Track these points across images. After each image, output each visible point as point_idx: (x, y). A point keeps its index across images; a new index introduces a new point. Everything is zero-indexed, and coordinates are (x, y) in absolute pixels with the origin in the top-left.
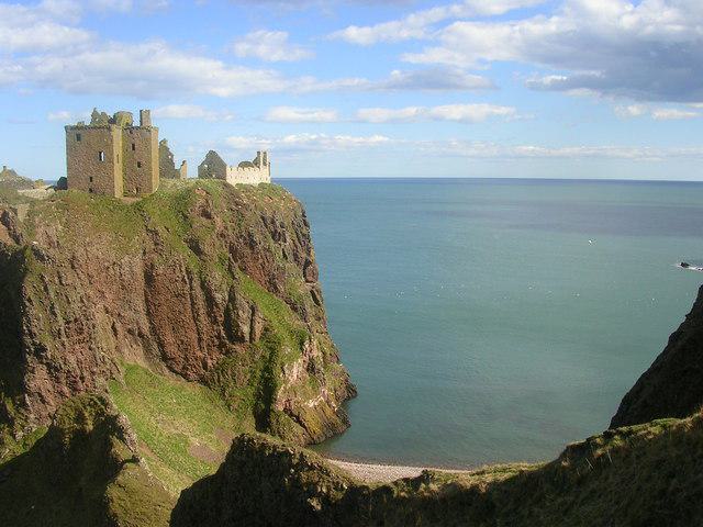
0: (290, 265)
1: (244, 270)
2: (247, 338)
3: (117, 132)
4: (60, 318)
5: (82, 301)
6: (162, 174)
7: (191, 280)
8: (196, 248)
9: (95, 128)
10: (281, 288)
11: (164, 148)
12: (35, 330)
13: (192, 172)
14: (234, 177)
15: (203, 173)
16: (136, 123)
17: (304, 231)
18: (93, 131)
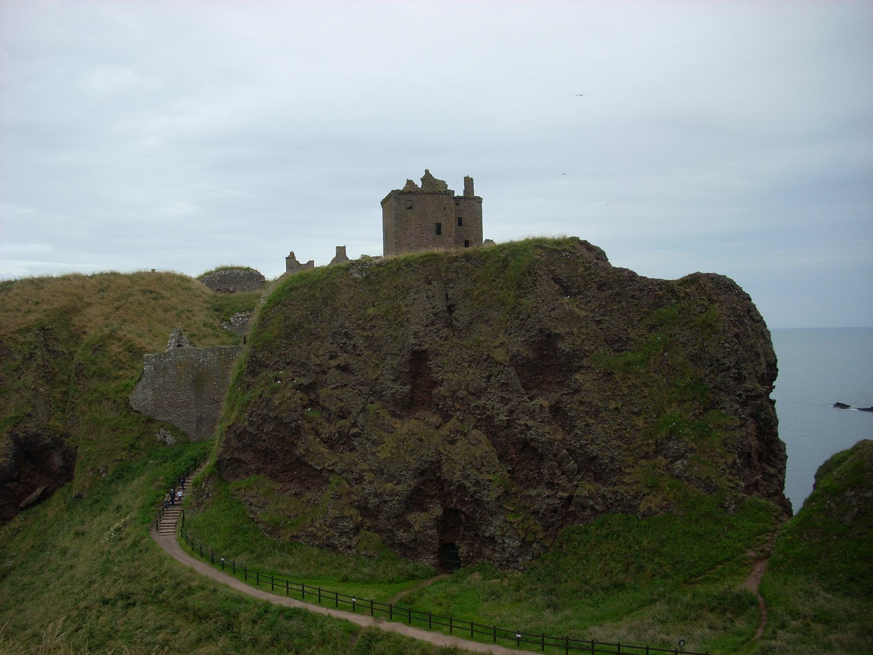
4: (762, 360)
16: (459, 192)
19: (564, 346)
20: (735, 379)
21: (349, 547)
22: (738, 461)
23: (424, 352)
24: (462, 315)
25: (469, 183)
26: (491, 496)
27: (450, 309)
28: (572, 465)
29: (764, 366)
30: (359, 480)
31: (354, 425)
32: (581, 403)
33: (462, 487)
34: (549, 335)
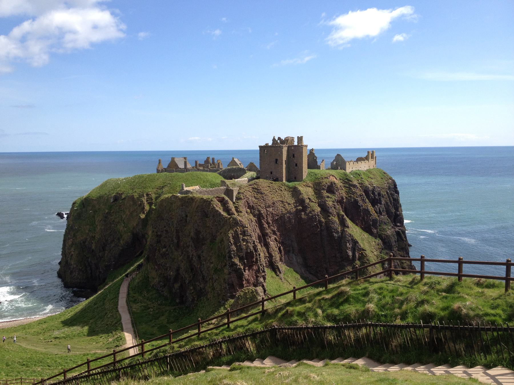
0: (384, 217)
2: (351, 257)
9: (274, 147)
10: (375, 231)
14: (350, 168)
15: (334, 167)
16: (296, 143)
17: (395, 197)
18: (273, 149)
20: (229, 257)
24: (188, 218)
25: (300, 139)
26: (187, 282)
30: (167, 269)
31: (167, 250)
32: (203, 257)
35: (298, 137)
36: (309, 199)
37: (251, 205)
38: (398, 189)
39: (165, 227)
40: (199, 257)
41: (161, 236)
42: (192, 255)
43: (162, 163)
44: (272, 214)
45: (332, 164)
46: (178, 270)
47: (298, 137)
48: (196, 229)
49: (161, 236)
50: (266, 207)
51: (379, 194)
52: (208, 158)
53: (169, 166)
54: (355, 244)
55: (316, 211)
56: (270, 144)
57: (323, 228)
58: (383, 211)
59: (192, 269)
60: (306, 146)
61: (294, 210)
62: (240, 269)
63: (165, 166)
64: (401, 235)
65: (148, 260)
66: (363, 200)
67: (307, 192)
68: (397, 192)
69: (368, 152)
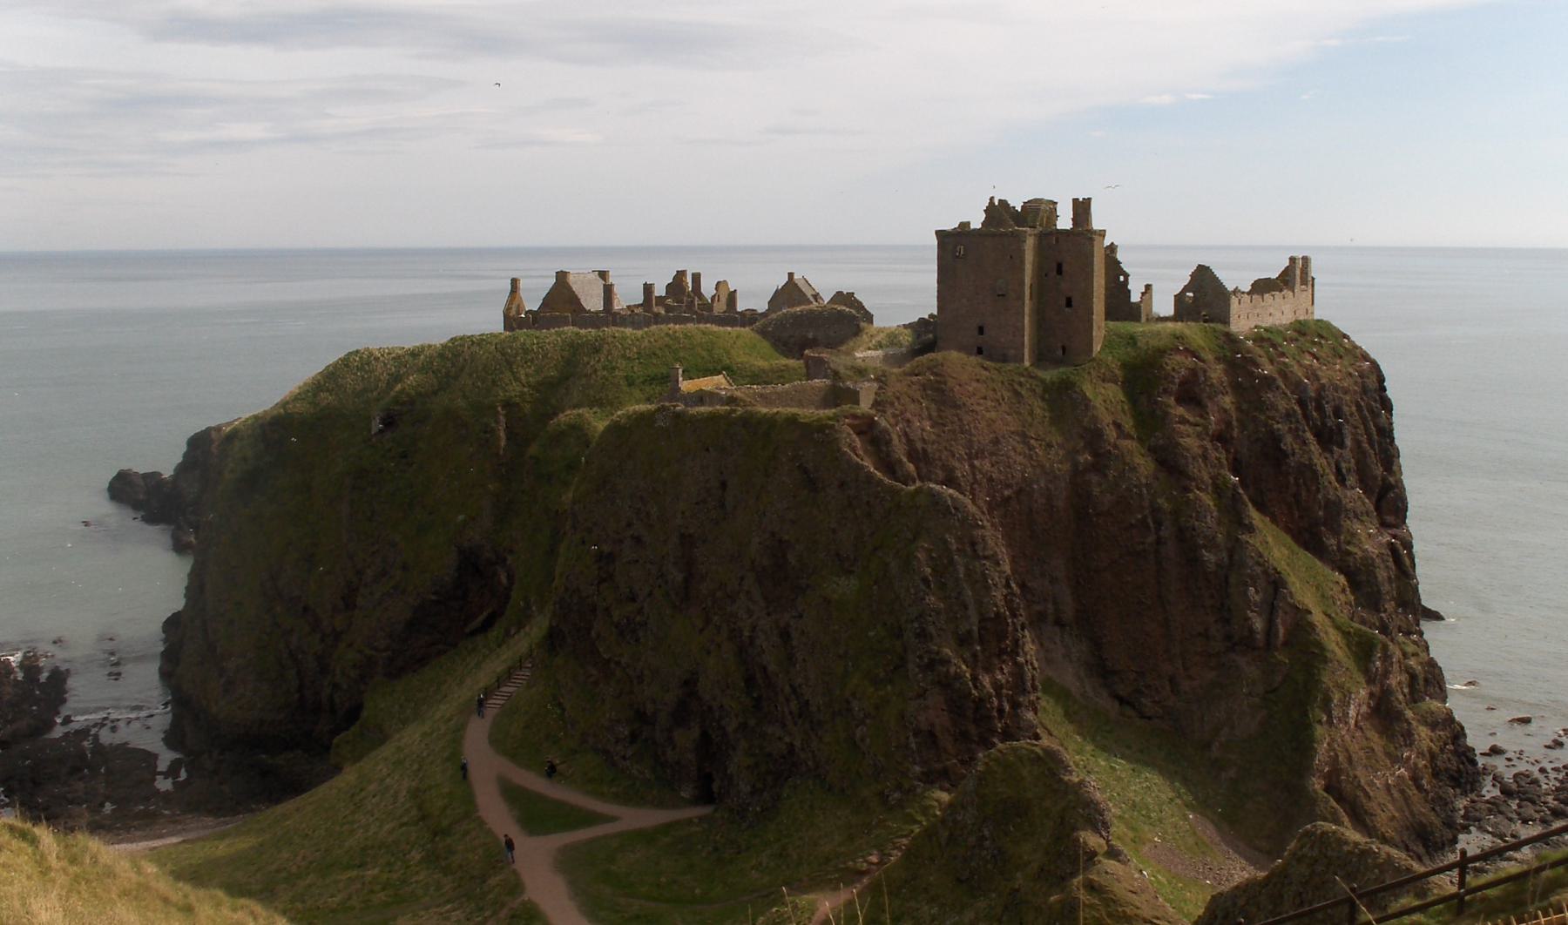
0: (1354, 496)
1: (1261, 507)
3: (1030, 243)
5: (1008, 586)
6: (1111, 314)
7: (1159, 524)
8: (1169, 462)
9: (994, 235)
10: (1331, 542)
11: (1114, 268)
12: (932, 629)
13: (1163, 305)
14: (1242, 321)
15: (1185, 308)
16: (1065, 222)
19: (792, 559)
20: (918, 636)
21: (624, 758)
22: (911, 739)
23: (690, 536)
25: (1082, 209)
27: (724, 485)
28: (794, 705)
29: (975, 619)
33: (710, 708)
34: (780, 541)
35: (1075, 201)
36: (1118, 426)
37: (919, 445)
38: (1389, 393)
39: (629, 525)
40: (785, 635)
41: (611, 557)
42: (754, 628)
43: (523, 293)
44: (991, 479)
45: (1179, 299)
46: (690, 683)
47: (1075, 201)
48: (773, 534)
49: (611, 557)
50: (970, 457)
51: (1338, 412)
52: (681, 274)
53: (548, 302)
54: (1276, 590)
55: (1142, 470)
56: (977, 221)
57: (1164, 533)
58: (1349, 470)
59: (750, 680)
60: (1102, 234)
61: (1066, 467)
62: (959, 676)
63: (532, 303)
64: (1401, 558)
65: (553, 640)
66: (1295, 433)
67: (1105, 399)
68: (1387, 405)
69: (1293, 260)
